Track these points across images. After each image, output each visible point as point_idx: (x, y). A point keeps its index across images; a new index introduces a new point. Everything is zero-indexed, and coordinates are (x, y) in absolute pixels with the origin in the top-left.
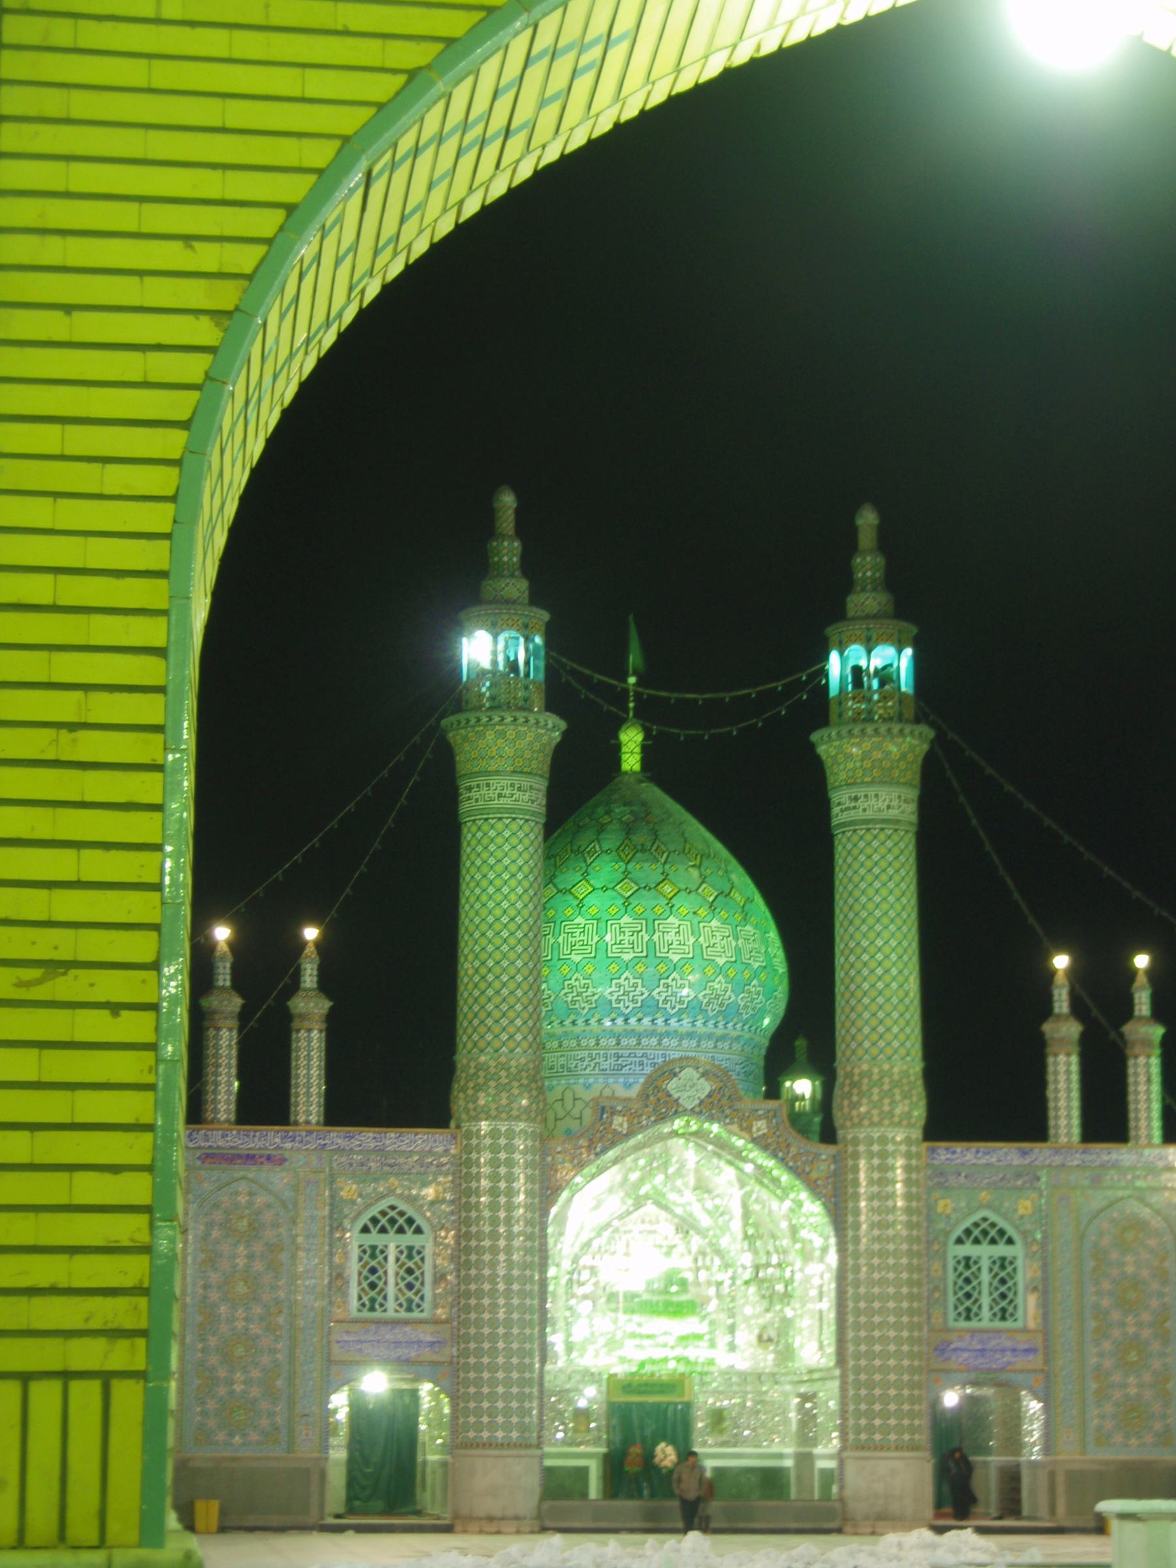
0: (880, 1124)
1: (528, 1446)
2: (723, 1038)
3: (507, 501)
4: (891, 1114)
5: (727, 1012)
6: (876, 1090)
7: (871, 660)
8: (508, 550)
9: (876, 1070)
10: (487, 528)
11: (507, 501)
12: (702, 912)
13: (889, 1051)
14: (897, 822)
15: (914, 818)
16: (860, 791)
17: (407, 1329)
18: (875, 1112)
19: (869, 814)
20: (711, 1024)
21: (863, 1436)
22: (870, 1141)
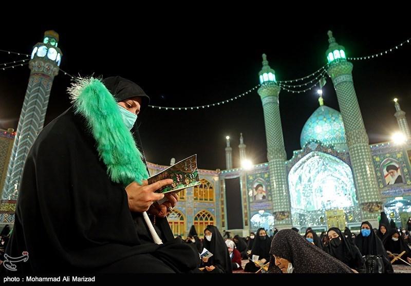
0: (355, 143)
1: (289, 224)
2: (342, 143)
3: (264, 56)
4: (357, 141)
5: (341, 138)
6: (353, 136)
7: (336, 55)
8: (265, 62)
9: (352, 132)
10: (262, 60)
11: (264, 56)
12: (332, 121)
13: (354, 127)
14: (346, 82)
15: (352, 80)
16: (337, 78)
17: (263, 203)
18: (353, 141)
19: (340, 82)
20: (338, 141)
21: (366, 216)
22: (354, 148)
